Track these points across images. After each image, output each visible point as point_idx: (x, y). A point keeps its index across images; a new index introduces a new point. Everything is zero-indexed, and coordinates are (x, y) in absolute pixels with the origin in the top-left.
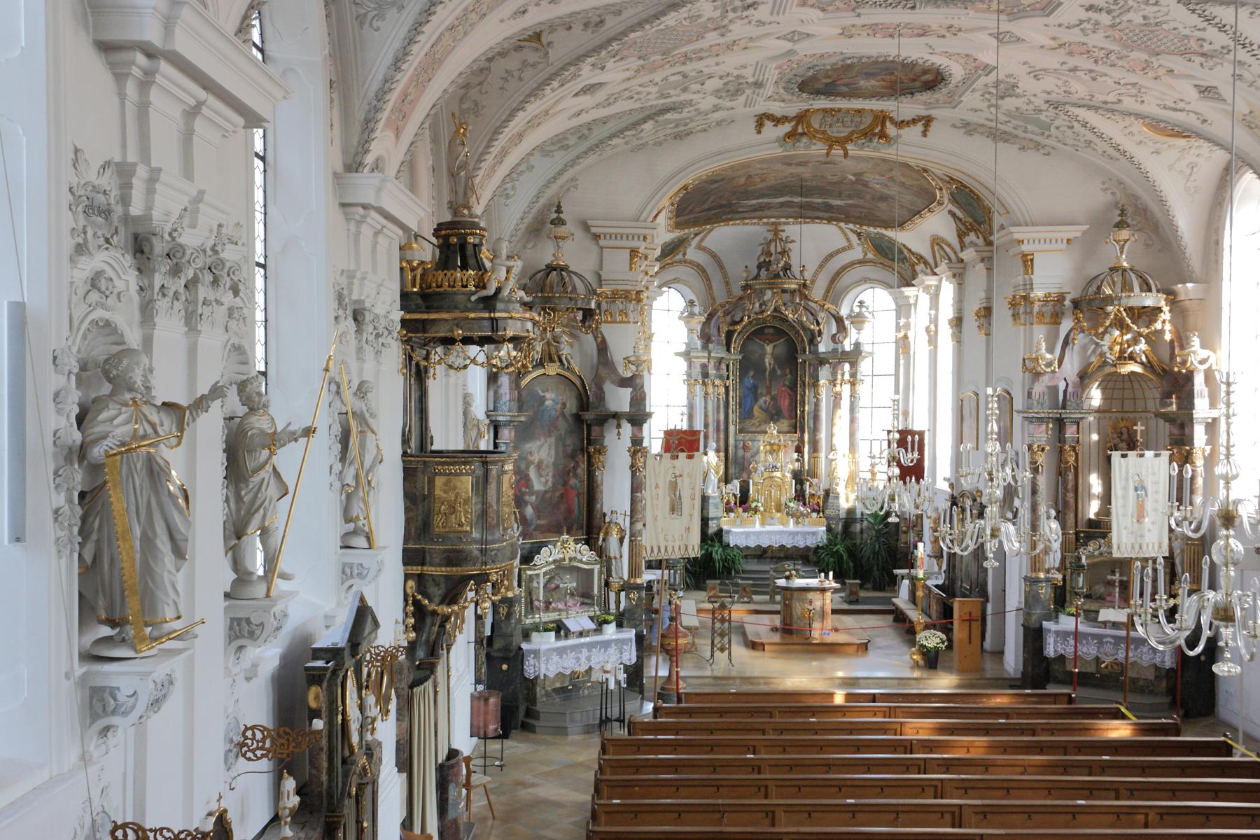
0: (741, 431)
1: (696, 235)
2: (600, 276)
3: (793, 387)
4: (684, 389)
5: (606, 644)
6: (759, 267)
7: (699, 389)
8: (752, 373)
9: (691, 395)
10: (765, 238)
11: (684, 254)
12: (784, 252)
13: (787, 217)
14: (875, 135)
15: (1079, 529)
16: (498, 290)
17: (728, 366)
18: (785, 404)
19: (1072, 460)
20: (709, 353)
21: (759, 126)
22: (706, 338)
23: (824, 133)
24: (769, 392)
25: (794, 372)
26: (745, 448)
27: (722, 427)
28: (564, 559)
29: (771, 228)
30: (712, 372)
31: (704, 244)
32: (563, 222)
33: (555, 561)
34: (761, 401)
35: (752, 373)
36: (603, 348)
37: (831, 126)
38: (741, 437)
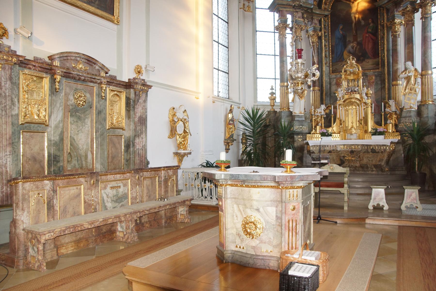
0: (333, 72)
3: (375, 33)
9: (282, 38)
17: (320, 21)
18: (369, 47)
24: (355, 39)
25: (375, 21)
34: (349, 47)
35: (341, 27)
38: (333, 76)
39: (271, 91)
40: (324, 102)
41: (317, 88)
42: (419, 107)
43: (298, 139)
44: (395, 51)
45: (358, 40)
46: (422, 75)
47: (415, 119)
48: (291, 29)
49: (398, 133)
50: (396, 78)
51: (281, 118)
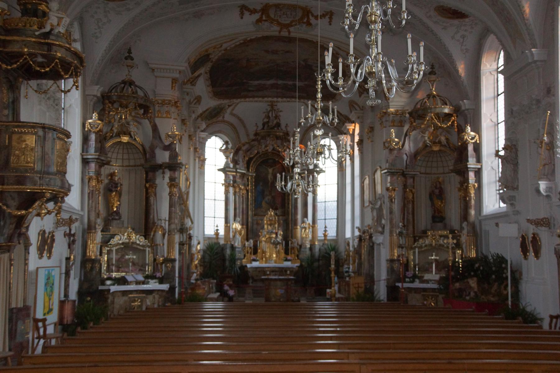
0: (255, 215)
1: (229, 106)
2: (155, 92)
4: (223, 189)
5: (149, 292)
6: (264, 124)
7: (231, 190)
8: (261, 184)
9: (227, 192)
10: (267, 109)
11: (223, 117)
12: (277, 117)
13: (277, 97)
14: (304, 23)
15: (416, 235)
16: (52, 30)
17: (248, 179)
19: (411, 197)
20: (236, 169)
21: (242, 15)
22: (235, 162)
23: (277, 21)
26: (258, 224)
27: (245, 212)
28: (129, 243)
29: (270, 104)
30: (238, 180)
31: (234, 112)
32: (132, 59)
33: (123, 244)
34: (266, 199)
35: (261, 184)
36: (155, 129)
37: (280, 16)
38: (255, 218)
39: (216, 228)
40: (249, 236)
41: (245, 226)
42: (311, 245)
43: (238, 263)
44: (296, 208)
45: (273, 194)
46: (312, 227)
47: (308, 252)
48: (233, 186)
49: (299, 261)
50: (296, 224)
51: (226, 249)
